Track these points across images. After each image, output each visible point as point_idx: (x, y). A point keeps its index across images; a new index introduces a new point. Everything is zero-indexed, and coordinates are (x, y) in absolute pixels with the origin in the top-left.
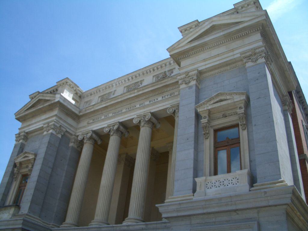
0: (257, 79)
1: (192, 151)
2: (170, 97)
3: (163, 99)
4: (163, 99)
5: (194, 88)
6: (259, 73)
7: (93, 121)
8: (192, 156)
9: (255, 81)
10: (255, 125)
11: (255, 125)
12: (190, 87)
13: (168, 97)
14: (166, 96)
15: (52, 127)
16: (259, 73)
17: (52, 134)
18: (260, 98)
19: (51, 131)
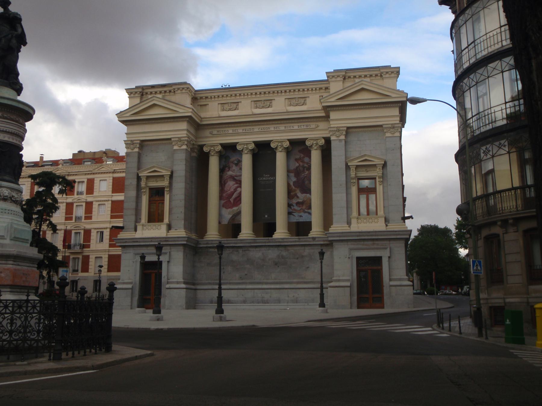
0: (393, 150)
1: (345, 195)
2: (306, 128)
3: (299, 128)
5: (343, 142)
6: (395, 145)
8: (345, 199)
9: (391, 151)
11: (390, 185)
12: (340, 140)
13: (304, 128)
14: (302, 126)
15: (186, 143)
16: (395, 145)
17: (186, 150)
18: (393, 165)
19: (184, 147)
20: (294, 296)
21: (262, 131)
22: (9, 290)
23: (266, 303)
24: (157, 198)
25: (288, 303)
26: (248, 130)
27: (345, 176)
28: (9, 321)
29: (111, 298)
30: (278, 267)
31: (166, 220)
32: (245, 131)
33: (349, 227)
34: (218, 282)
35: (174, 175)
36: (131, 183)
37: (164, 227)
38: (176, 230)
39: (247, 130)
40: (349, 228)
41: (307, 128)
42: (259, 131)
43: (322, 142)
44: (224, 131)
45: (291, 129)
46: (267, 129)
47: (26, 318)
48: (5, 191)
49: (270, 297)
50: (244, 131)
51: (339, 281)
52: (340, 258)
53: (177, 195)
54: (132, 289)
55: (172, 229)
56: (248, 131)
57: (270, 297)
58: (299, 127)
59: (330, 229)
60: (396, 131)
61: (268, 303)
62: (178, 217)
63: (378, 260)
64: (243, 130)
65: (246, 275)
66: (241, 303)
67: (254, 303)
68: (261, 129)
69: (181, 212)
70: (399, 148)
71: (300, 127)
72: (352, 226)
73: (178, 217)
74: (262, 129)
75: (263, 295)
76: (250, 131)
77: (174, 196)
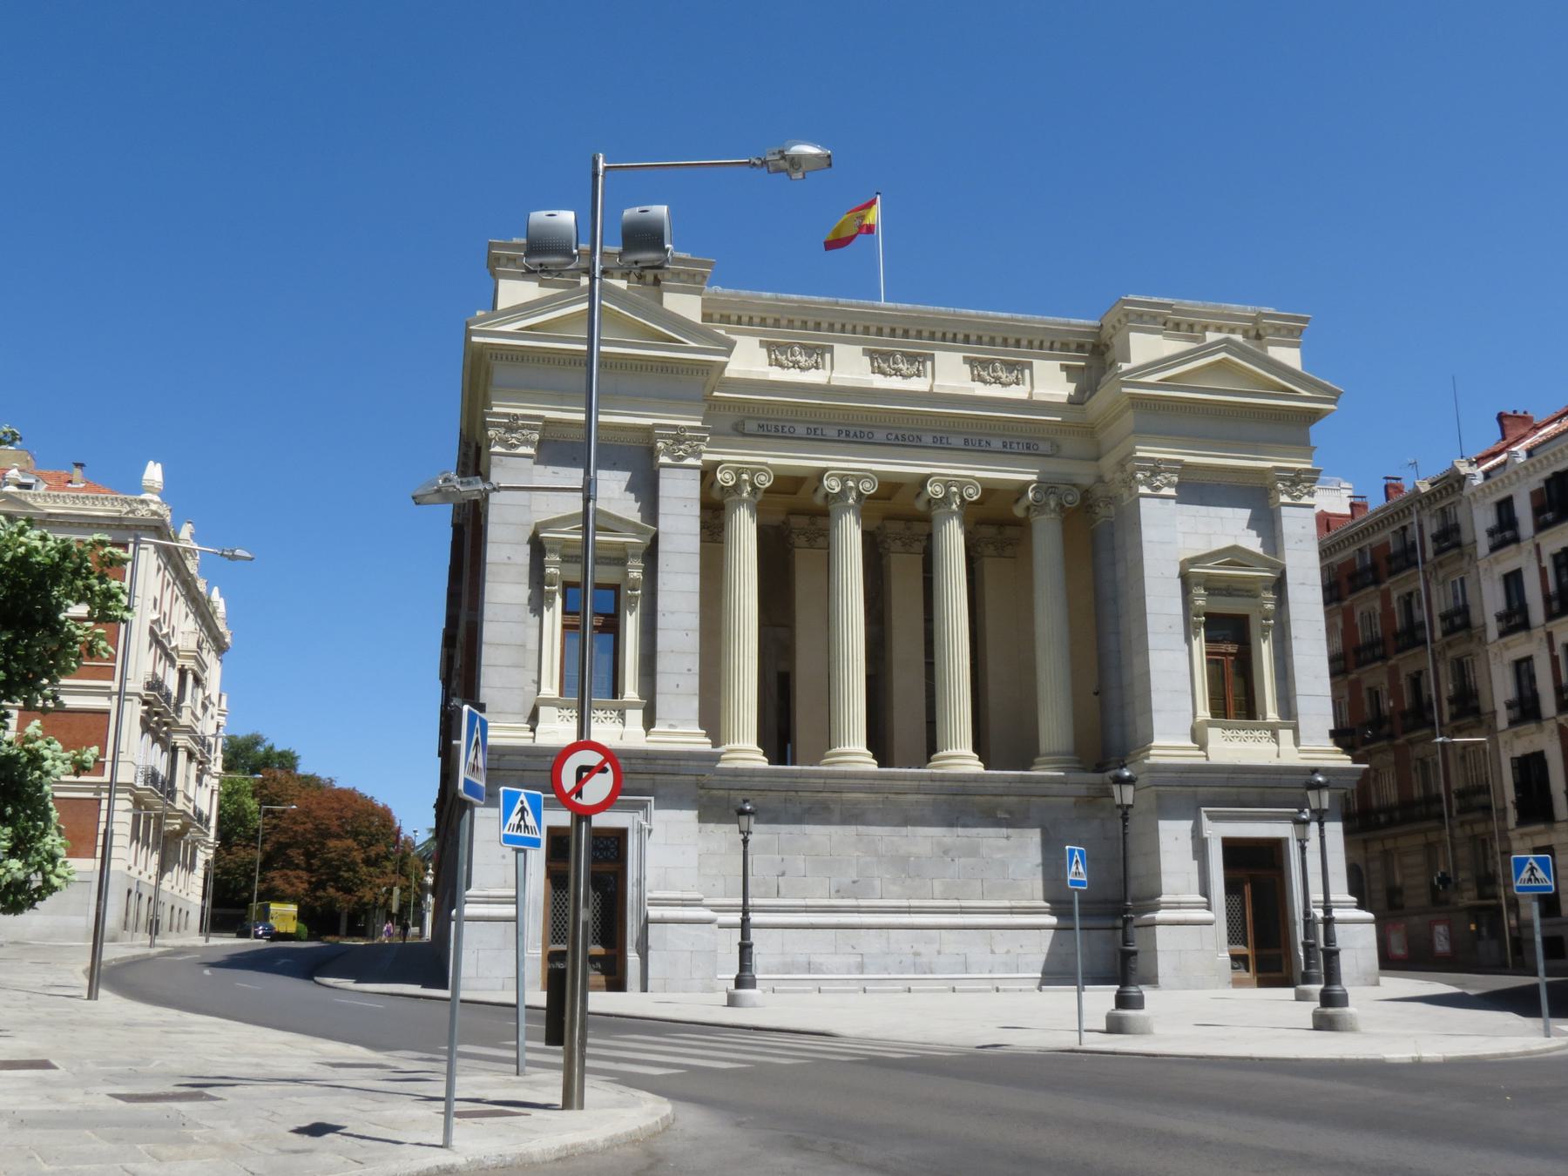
0: (1301, 541)
3: (1005, 450)
4: (1005, 450)
6: (1303, 527)
7: (761, 432)
10: (1296, 637)
14: (1015, 445)
18: (1303, 584)
20: (1008, 952)
21: (897, 442)
23: (925, 973)
25: (990, 972)
26: (855, 435)
27: (1179, 601)
30: (953, 860)
32: (847, 435)
33: (1200, 749)
34: (740, 901)
35: (662, 546)
36: (509, 558)
38: (671, 726)
39: (851, 435)
40: (1202, 753)
41: (1028, 452)
42: (889, 442)
43: (1073, 499)
44: (780, 429)
45: (983, 448)
46: (911, 439)
49: (939, 953)
50: (843, 437)
51: (1178, 906)
52: (1176, 839)
53: (672, 613)
54: (516, 919)
55: (657, 722)
56: (855, 439)
57: (939, 953)
58: (1004, 446)
59: (1152, 752)
60: (1305, 491)
61: (932, 973)
62: (678, 686)
63: (1275, 848)
64: (840, 432)
65: (854, 882)
66: (849, 973)
67: (889, 974)
68: (893, 437)
69: (689, 670)
70: (1313, 539)
71: (1008, 446)
72: (1210, 746)
73: (678, 686)
74: (897, 437)
75: (915, 945)
76: (862, 440)
77: (664, 615)
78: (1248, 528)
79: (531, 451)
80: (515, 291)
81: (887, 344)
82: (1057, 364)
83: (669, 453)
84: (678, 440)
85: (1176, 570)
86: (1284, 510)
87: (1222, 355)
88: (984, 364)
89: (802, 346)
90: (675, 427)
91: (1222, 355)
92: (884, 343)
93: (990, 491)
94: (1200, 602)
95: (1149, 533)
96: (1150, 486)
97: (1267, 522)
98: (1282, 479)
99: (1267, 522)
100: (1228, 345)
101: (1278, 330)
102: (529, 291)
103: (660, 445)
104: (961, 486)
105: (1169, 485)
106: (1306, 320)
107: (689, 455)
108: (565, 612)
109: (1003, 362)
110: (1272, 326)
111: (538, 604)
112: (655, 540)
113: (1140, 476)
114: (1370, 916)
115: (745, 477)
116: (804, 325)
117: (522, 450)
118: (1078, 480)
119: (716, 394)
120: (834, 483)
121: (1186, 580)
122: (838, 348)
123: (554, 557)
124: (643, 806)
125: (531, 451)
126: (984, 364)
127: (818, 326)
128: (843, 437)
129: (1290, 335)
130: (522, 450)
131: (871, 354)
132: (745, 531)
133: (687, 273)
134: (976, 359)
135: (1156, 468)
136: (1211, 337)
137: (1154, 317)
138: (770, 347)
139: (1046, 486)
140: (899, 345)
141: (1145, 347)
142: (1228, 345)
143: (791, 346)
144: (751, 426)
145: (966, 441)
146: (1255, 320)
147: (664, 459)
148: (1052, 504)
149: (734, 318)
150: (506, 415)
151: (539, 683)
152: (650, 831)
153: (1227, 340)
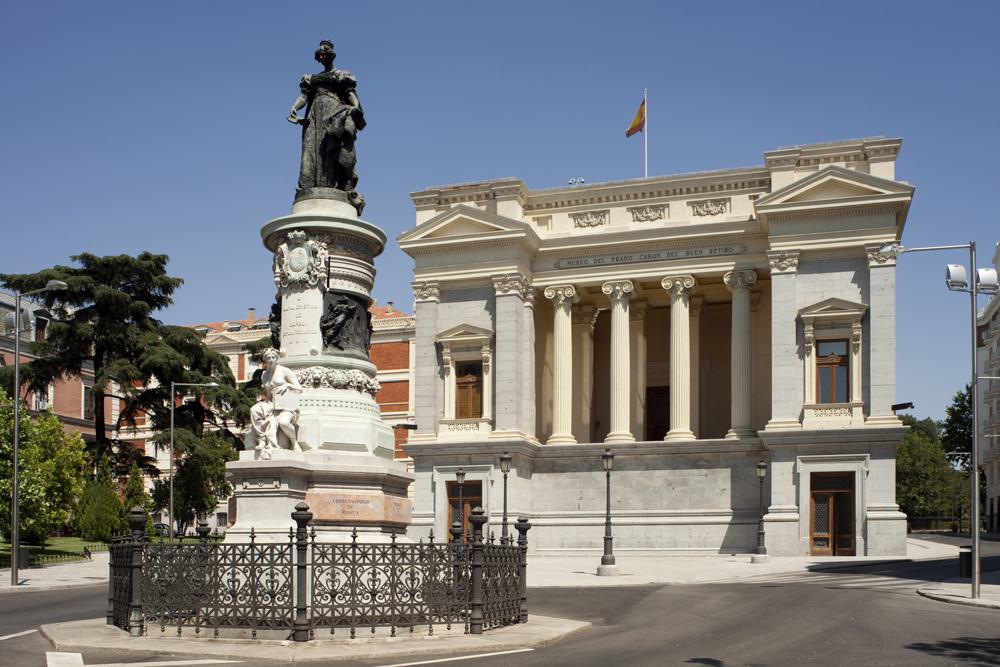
22: (380, 529)
24: (470, 378)
28: (409, 575)
29: (522, 541)
31: (487, 414)
35: (498, 338)
37: (485, 427)
43: (751, 278)
47: (354, 573)
48: (359, 375)
78: (852, 282)
79: (433, 298)
80: (424, 216)
81: (641, 202)
82: (747, 196)
83: (500, 289)
84: (504, 282)
85: (795, 316)
86: (872, 271)
87: (829, 177)
88: (700, 204)
89: (592, 213)
90: (501, 275)
91: (829, 177)
92: (640, 203)
93: (700, 279)
94: (809, 335)
95: (776, 297)
96: (778, 267)
97: (863, 280)
98: (871, 251)
99: (863, 280)
100: (832, 171)
101: (877, 151)
102: (430, 214)
103: (496, 286)
104: (683, 279)
105: (792, 265)
106: (900, 141)
107: (510, 289)
108: (459, 374)
109: (712, 201)
110: (872, 149)
111: (443, 373)
112: (494, 337)
113: (772, 263)
114: (905, 515)
115: (560, 292)
116: (592, 200)
117: (430, 299)
118: (757, 266)
119: (541, 249)
120: (608, 289)
121: (800, 323)
122: (612, 210)
123: (446, 350)
124: (488, 469)
125: (433, 298)
126: (700, 204)
127: (600, 200)
128: (615, 262)
129: (891, 151)
130: (430, 299)
131: (632, 210)
132: (563, 321)
133: (509, 190)
134: (696, 202)
135: (782, 256)
136: (822, 167)
137: (788, 160)
138: (575, 216)
139: (733, 274)
140: (648, 202)
141: (781, 179)
142: (832, 171)
143: (586, 214)
144: (564, 264)
145: (687, 253)
146: (862, 148)
147: (498, 293)
148: (740, 283)
149: (554, 204)
150: (420, 283)
151: (444, 413)
152: (492, 482)
153: (832, 167)
